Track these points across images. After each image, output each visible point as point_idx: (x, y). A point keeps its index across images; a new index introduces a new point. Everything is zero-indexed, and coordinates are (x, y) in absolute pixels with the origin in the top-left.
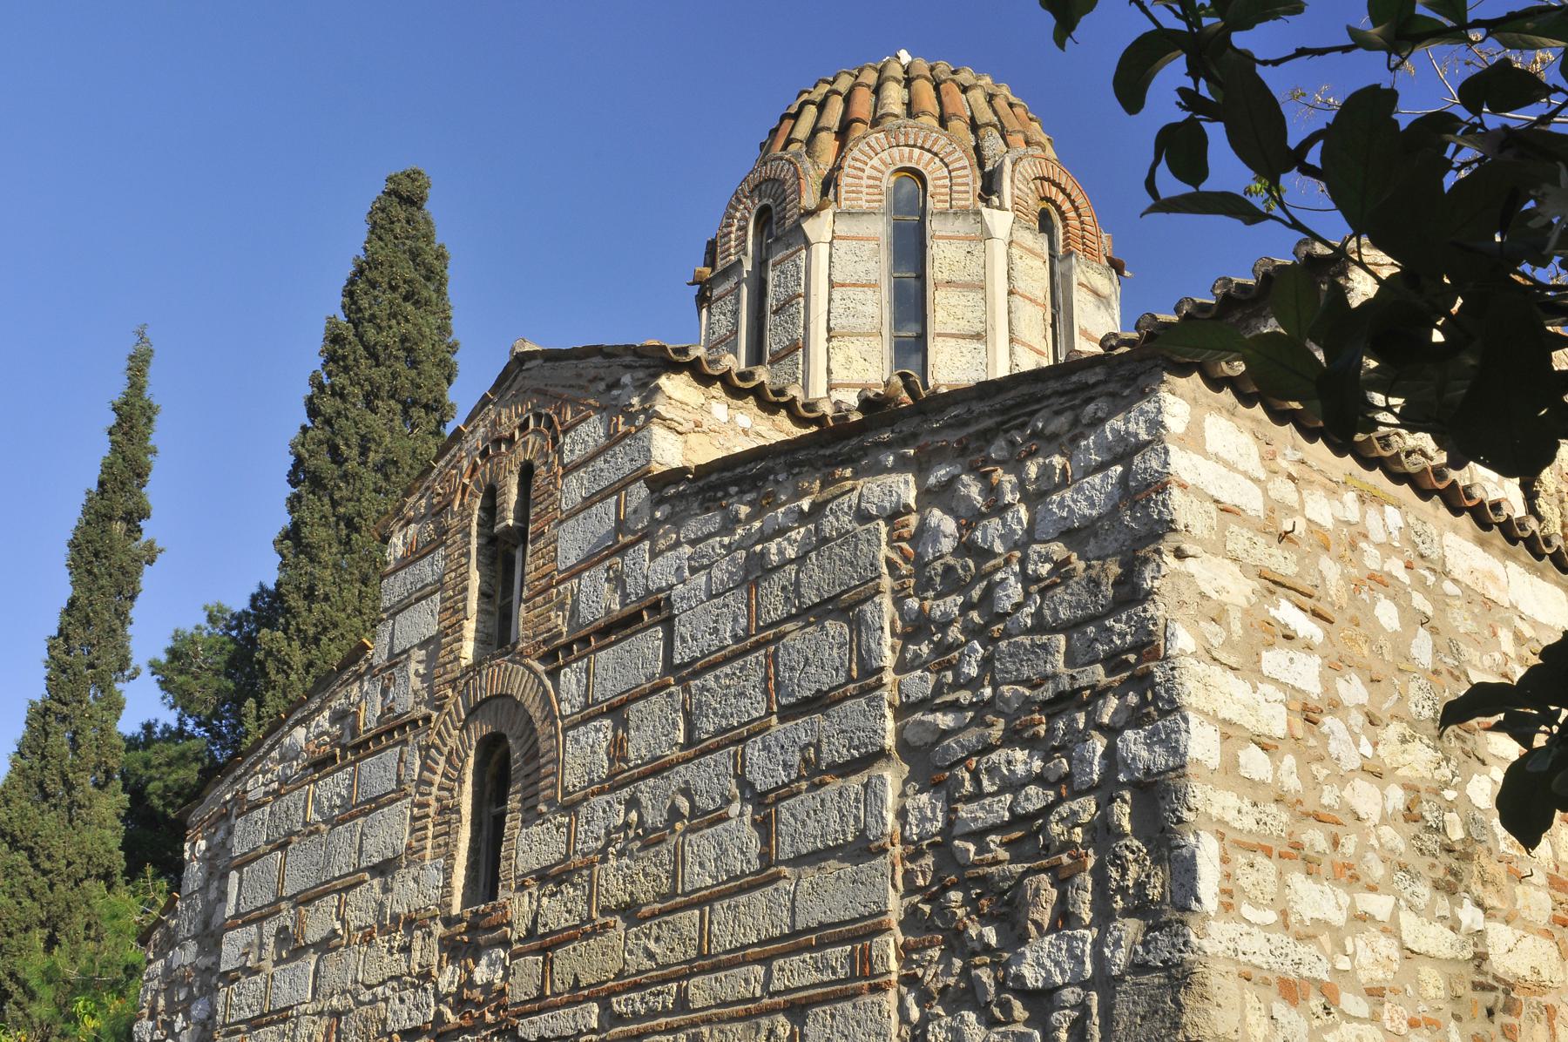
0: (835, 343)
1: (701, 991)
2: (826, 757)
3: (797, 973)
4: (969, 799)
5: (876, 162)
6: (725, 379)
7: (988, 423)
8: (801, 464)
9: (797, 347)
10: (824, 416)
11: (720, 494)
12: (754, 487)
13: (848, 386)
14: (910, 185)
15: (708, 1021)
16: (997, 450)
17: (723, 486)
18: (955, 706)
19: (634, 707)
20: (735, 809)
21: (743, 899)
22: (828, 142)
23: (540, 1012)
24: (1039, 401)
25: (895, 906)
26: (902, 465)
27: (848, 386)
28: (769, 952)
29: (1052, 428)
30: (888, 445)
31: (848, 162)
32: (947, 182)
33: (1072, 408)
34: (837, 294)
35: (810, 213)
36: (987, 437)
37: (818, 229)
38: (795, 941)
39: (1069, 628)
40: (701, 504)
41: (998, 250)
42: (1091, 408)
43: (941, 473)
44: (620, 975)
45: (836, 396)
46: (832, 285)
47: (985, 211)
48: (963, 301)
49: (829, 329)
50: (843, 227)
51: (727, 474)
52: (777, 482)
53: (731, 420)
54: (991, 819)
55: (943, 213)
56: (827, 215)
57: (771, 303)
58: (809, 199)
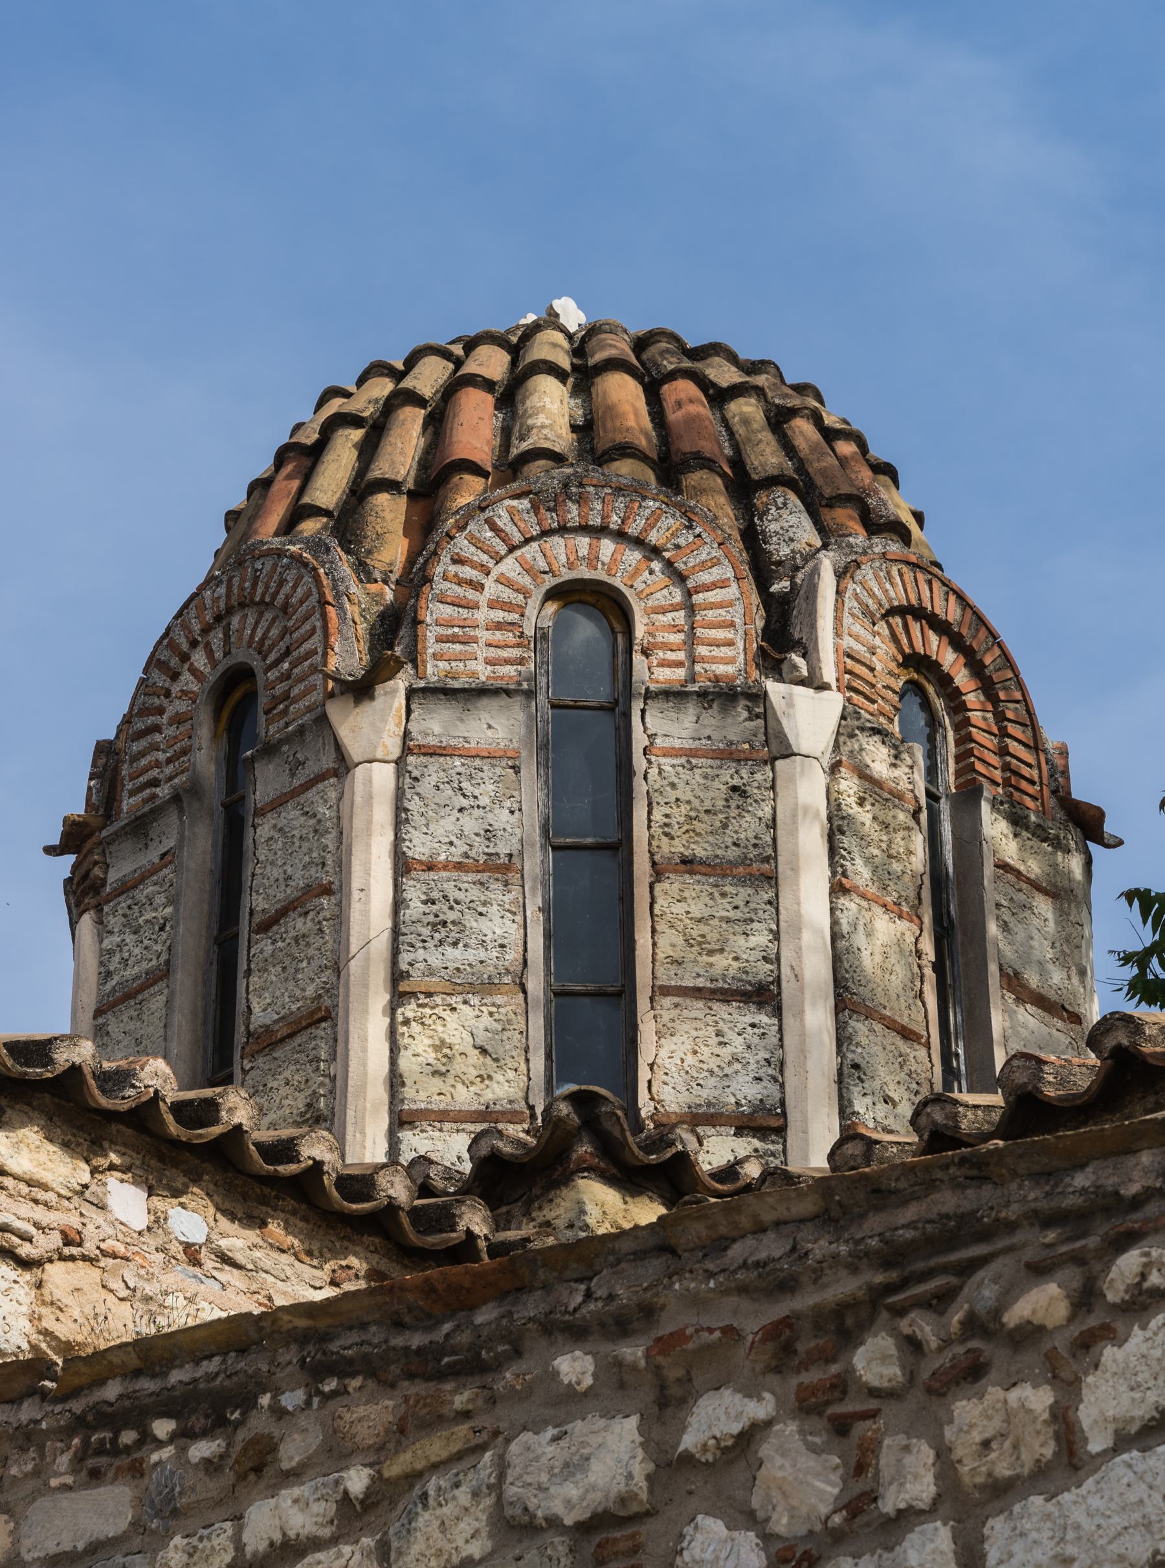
0: (409, 1010)
5: (509, 567)
6: (143, 1117)
7: (845, 1287)
8: (343, 1368)
9: (322, 1017)
10: (392, 1207)
11: (128, 1437)
12: (218, 1424)
13: (442, 1117)
14: (586, 629)
16: (874, 1361)
17: (136, 1414)
22: (389, 513)
24: (985, 1235)
26: (615, 1385)
27: (442, 1117)
29: (1022, 1310)
30: (576, 1333)
31: (443, 566)
32: (680, 617)
33: (1078, 1259)
34: (414, 893)
35: (361, 690)
36: (844, 1326)
37: (373, 730)
40: (79, 1459)
41: (807, 788)
42: (1129, 1262)
43: (716, 1416)
45: (415, 1143)
46: (402, 866)
47: (775, 689)
48: (723, 909)
49: (397, 976)
50: (434, 724)
51: (148, 1385)
52: (279, 1413)
53: (158, 1222)
55: (672, 696)
56: (393, 693)
57: (259, 900)
58: (348, 656)
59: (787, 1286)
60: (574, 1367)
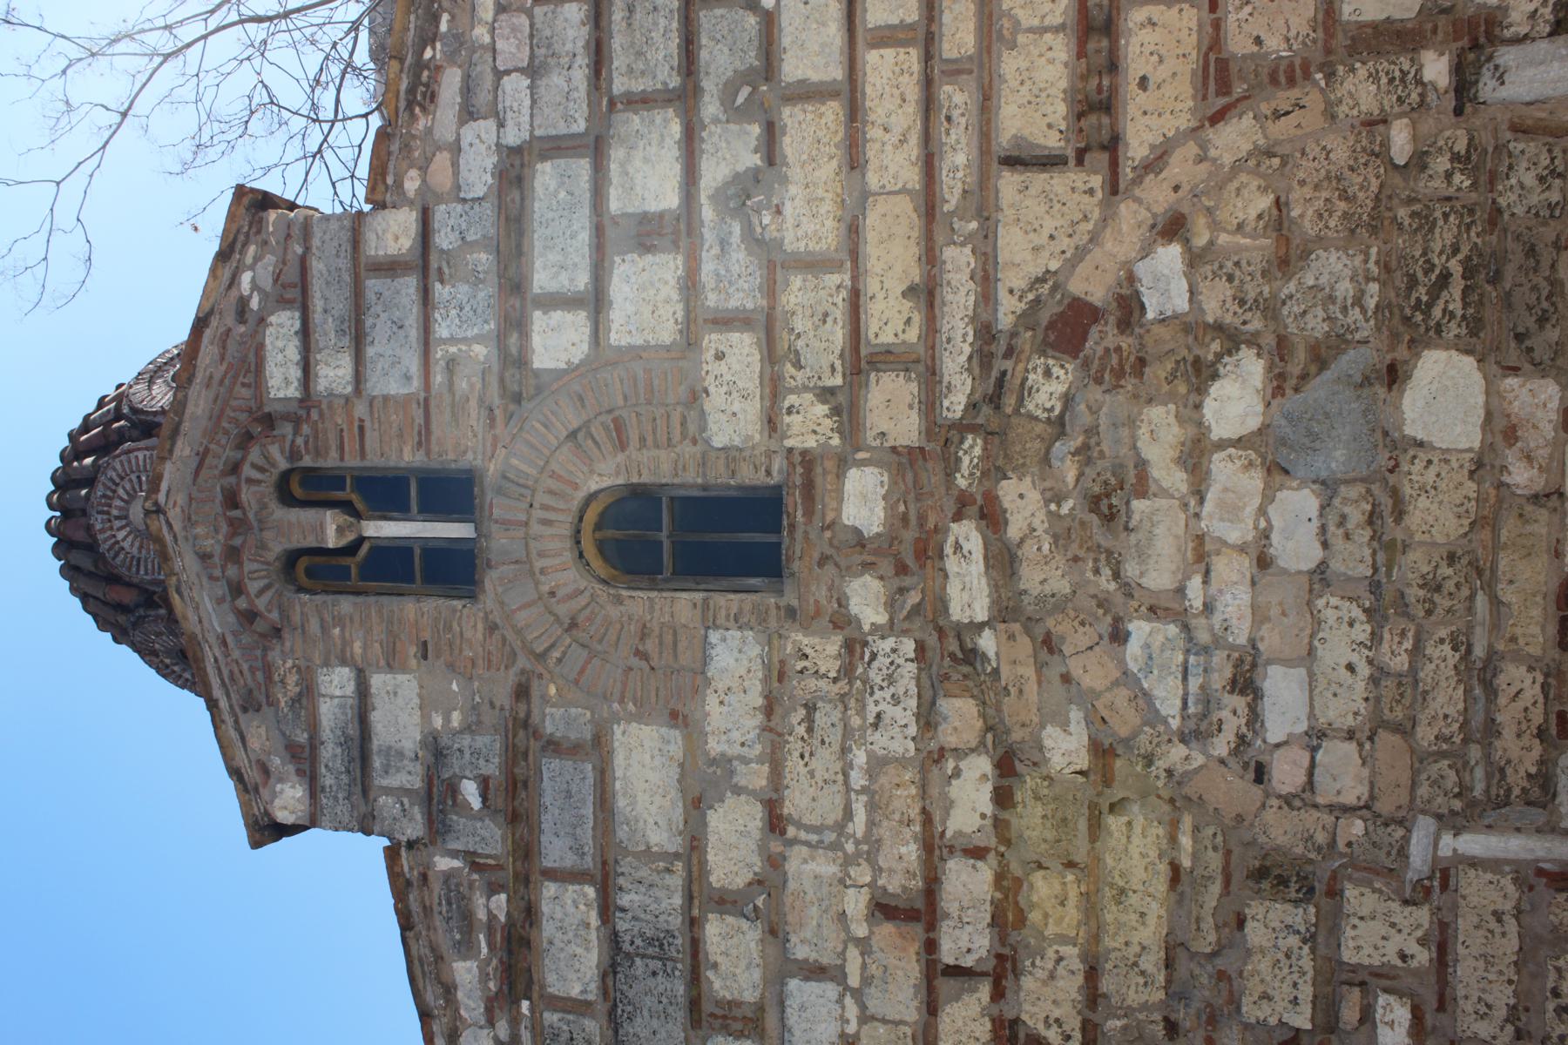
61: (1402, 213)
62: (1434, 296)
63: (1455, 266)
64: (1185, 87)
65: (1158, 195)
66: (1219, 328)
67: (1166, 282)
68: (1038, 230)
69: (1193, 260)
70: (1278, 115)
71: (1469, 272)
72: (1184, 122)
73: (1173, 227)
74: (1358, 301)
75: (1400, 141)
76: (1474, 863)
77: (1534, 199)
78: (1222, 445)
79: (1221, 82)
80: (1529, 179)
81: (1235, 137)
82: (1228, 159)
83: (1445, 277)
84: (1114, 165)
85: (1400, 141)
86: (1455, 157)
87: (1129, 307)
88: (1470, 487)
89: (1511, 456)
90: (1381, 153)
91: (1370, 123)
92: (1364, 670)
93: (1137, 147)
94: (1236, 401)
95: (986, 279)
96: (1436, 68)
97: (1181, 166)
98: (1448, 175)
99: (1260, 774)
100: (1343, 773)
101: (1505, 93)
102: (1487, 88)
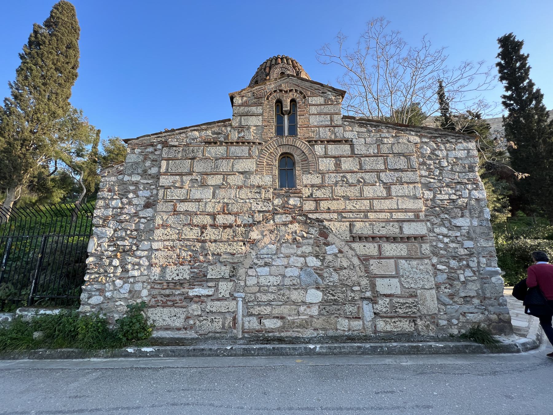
1: (371, 216)
2: (403, 180)
3: (401, 216)
4: (438, 194)
15: (375, 221)
18: (434, 179)
19: (343, 159)
20: (378, 184)
21: (383, 201)
23: (316, 213)
25: (424, 208)
28: (391, 211)
38: (398, 210)
39: (458, 172)
44: (344, 209)
54: (445, 198)
59: (432, 134)
60: (413, 133)
61: (344, 289)
62: (332, 294)
63: (336, 297)
64: (364, 253)
65: (346, 249)
66: (324, 259)
67: (331, 250)
68: (339, 228)
69: (336, 255)
70: (360, 268)
71: (335, 300)
72: (358, 253)
73: (340, 252)
74: (330, 282)
75: (357, 288)
76: (237, 304)
77: (347, 310)
78: (305, 259)
79: (365, 259)
80: (351, 309)
81: (356, 261)
82: (352, 260)
83: (334, 296)
84: (351, 242)
85: (357, 288)
86: (354, 297)
87: (327, 244)
88: (300, 301)
89: (305, 307)
90: (354, 286)
91: (359, 283)
92: (269, 284)
93: (354, 245)
94: (313, 262)
95: (330, 220)
96: (368, 294)
97: (351, 252)
98: (351, 296)
99: (251, 268)
100: (252, 281)
101: (364, 305)
102: (365, 302)
